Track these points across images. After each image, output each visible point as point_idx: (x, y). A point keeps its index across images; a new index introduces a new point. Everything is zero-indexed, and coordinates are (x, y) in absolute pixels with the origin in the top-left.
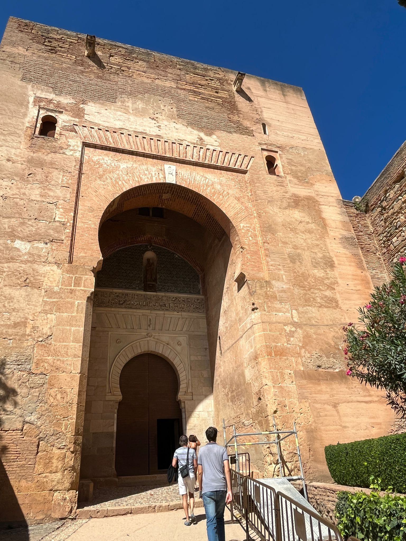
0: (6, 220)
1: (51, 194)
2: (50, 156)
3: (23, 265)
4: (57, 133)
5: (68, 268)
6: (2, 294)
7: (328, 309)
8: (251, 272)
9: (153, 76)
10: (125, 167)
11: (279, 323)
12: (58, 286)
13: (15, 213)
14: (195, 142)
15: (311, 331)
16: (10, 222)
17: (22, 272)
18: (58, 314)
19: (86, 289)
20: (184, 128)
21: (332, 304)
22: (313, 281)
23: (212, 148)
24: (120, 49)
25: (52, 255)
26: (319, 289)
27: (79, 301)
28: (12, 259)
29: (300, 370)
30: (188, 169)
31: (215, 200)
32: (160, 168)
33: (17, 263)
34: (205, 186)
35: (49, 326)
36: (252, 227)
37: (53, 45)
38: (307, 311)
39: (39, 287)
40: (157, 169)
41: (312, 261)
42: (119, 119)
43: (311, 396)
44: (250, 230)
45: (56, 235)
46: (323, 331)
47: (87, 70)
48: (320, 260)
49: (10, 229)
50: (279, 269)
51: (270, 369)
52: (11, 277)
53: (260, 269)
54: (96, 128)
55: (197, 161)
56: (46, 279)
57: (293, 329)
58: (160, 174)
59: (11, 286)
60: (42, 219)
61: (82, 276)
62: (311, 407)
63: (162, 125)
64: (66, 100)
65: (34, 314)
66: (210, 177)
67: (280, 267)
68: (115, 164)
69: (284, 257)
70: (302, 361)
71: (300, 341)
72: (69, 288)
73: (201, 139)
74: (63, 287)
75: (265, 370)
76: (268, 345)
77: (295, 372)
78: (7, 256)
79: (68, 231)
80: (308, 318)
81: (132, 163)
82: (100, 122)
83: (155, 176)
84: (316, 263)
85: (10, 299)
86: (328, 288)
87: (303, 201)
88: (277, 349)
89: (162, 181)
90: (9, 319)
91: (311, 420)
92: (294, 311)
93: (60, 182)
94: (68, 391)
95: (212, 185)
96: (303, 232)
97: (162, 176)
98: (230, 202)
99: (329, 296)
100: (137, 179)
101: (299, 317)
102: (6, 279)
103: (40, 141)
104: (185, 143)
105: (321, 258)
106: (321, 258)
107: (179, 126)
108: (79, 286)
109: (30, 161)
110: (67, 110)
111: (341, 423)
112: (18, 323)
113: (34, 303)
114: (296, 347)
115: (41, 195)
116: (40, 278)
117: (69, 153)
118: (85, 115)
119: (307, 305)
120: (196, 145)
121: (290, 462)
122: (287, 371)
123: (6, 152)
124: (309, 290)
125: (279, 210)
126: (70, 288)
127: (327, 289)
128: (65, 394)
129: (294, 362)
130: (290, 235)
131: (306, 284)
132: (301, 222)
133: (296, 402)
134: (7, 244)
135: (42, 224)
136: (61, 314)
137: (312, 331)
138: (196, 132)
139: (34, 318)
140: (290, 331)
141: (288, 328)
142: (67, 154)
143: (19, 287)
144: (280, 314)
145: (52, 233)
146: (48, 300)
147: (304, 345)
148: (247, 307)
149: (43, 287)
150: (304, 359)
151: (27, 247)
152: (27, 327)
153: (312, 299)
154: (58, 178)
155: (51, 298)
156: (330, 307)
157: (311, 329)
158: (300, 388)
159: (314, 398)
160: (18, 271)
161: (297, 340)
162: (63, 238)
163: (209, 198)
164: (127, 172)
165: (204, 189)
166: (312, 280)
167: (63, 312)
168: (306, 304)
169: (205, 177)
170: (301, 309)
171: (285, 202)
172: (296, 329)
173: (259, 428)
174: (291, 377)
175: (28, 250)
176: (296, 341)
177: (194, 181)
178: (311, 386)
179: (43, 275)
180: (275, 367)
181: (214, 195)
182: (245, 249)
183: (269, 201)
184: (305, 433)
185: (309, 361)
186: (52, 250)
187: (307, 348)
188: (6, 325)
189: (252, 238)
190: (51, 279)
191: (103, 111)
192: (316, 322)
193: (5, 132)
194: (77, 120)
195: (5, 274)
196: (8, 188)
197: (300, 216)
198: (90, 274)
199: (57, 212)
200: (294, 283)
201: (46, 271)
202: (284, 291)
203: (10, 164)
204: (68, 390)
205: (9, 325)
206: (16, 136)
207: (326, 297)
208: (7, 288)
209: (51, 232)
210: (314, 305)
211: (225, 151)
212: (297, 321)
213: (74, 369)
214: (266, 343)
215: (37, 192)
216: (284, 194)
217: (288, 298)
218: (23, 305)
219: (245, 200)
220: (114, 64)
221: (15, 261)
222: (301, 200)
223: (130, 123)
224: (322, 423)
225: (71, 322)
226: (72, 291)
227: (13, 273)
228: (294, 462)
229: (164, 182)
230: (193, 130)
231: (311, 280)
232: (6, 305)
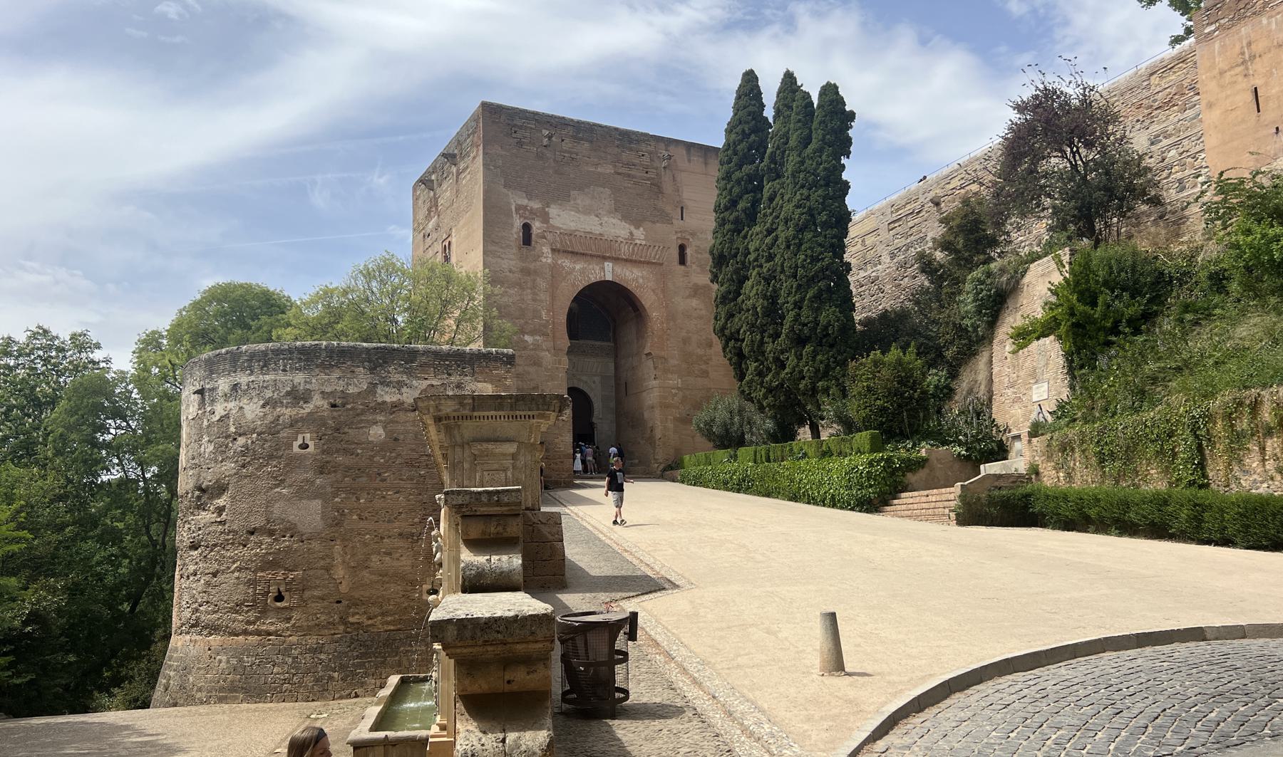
9: (596, 160)
24: (569, 128)
31: (637, 293)
37: (518, 135)
47: (546, 165)
64: (536, 205)
73: (631, 233)
103: (524, 250)
107: (614, 221)
110: (537, 216)
138: (627, 226)
191: (561, 213)
203: (511, 274)
211: (648, 244)
215: (530, 297)
220: (566, 151)
226: (557, 368)
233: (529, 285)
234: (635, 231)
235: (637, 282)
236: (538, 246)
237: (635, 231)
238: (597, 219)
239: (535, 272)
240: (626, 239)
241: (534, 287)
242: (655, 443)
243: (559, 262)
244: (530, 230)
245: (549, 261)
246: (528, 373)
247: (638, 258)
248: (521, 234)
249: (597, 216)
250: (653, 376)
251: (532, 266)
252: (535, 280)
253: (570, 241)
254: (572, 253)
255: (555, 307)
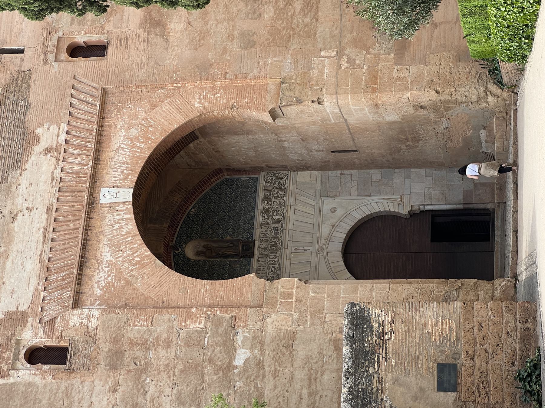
0: (207, 378)
1: (164, 336)
2: (102, 345)
3: (267, 352)
4: (59, 342)
5: (269, 307)
6: (302, 367)
7: (319, 9)
8: (268, 100)
10: (110, 253)
11: (337, 74)
12: (292, 315)
13: (196, 371)
14: (54, 159)
15: (348, 37)
16: (209, 375)
17: (275, 352)
18: (325, 311)
19: (295, 286)
20: (26, 174)
21: (313, 3)
22: (281, 22)
23: (63, 137)
25: (253, 325)
26: (292, 16)
27: (311, 292)
28: (260, 365)
29: (394, 58)
30: (105, 171)
32: (106, 209)
33: (265, 358)
34: (134, 149)
35: (339, 318)
36: (200, 91)
38: (322, 37)
39: (294, 333)
40: (109, 213)
41: (251, 19)
42: (22, 265)
43: (423, 50)
44: (204, 94)
45: (225, 324)
46: (348, 22)
48: (249, 7)
49: (220, 372)
50: (265, 64)
51: (392, 92)
52: (282, 362)
53: (263, 89)
54: (43, 294)
55: (90, 158)
56: (283, 328)
57: (345, 58)
58: (118, 208)
59: (292, 360)
60: (203, 342)
61: (279, 292)
62: (434, 52)
63: (26, 205)
65: (325, 334)
66: (116, 141)
67: (262, 62)
68: (106, 267)
69: (246, 54)
70: (383, 54)
71: (360, 52)
72: (294, 304)
73: (47, 151)
74: (293, 310)
75: (392, 98)
76: (364, 90)
77: (397, 64)
78: (256, 369)
79: (218, 312)
80: (332, 37)
81: (101, 246)
82: (32, 289)
83: (123, 215)
84: (254, 13)
85: (309, 359)
86: (291, 5)
87: (152, 13)
88: (369, 80)
89: (131, 206)
90: (330, 356)
91: (447, 54)
92: (322, 54)
93: (145, 328)
94: (407, 293)
95: (131, 140)
96: (206, 23)
97: (121, 206)
98: (159, 118)
99: (303, 6)
100: (130, 238)
101: (330, 48)
102: (284, 365)
103: (75, 361)
104: (58, 174)
105: (247, 5)
106: (247, 5)
107: (24, 181)
108: (292, 294)
109: (113, 367)
110: (13, 335)
111: (453, 22)
112: (335, 347)
113: (313, 335)
114: (368, 59)
115: (168, 347)
116: (282, 334)
117: (94, 323)
118: (20, 309)
119: (315, 36)
120: (61, 159)
121: (486, 83)
122: (394, 73)
123: (101, 396)
124: (293, 29)
125: (170, 51)
126: (294, 302)
127: (292, 6)
128: (410, 296)
129: (385, 64)
130: (211, 41)
131: (284, 32)
132: (189, 23)
133: (428, 68)
134: (240, 372)
135: (210, 341)
136: (325, 308)
137: (348, 36)
138: (33, 158)
139: (329, 333)
140: (348, 62)
141: (344, 65)
142: (96, 325)
143: (294, 353)
144: (326, 71)
145: (223, 329)
146: (309, 323)
147: (366, 49)
148: (313, 110)
149: (294, 329)
150: (382, 52)
151: (243, 352)
152: (339, 338)
153: (306, 29)
154: (139, 332)
155: (306, 320)
156: (317, 7)
157: (346, 37)
158: (414, 62)
159: (426, 47)
160: (274, 356)
161: (359, 56)
162: (228, 316)
163: (154, 146)
164: (118, 251)
165: (139, 151)
166: (279, 23)
167: (324, 307)
168: (313, 37)
169: (118, 149)
170: (320, 45)
171: (155, 40)
172: (345, 55)
173: (452, 111)
174: (402, 69)
175: (247, 351)
176: (360, 58)
177: (127, 164)
178: (412, 48)
179: (279, 331)
180: (390, 86)
181: (150, 139)
182: (235, 104)
183: (157, 63)
184: (460, 63)
185: (384, 46)
186: (245, 326)
187: (368, 45)
188: (337, 357)
189: (217, 93)
190: (284, 322)
192: (336, 28)
193: (64, 404)
194: (30, 319)
195: (278, 368)
196: (160, 384)
197: (180, 22)
198: (277, 283)
199: (191, 327)
200: (284, 48)
201: (274, 329)
202: (296, 63)
203: (121, 389)
204: (406, 293)
205: (338, 354)
206: (72, 390)
207: (302, 10)
208: (295, 363)
209: (221, 330)
210: (314, 27)
211: (69, 118)
212: (335, 53)
213: (385, 290)
214: (362, 93)
215: (162, 352)
216: (141, 39)
217: (305, 58)
218: (314, 346)
219: (155, 97)
221: (261, 361)
222: (150, 15)
223: (26, 250)
224: (452, 43)
225: (335, 298)
226: (298, 301)
227: (276, 360)
228: (487, 79)
229: (132, 203)
230: (30, 162)
231: (280, 25)
232: (315, 361)
233: (139, 353)
234: (43, 144)
235: (137, 138)
236: (70, 334)
237: (43, 144)
238: (19, 217)
239: (115, 341)
240: (58, 161)
241: (145, 345)
242: (446, 102)
243: (98, 292)
244: (41, 348)
245: (96, 313)
246: (308, 358)
247: (93, 137)
248: (46, 367)
249: (14, 218)
250: (316, 106)
251: (105, 347)
252: (131, 342)
253: (60, 270)
254: (81, 266)
255: (180, 303)
